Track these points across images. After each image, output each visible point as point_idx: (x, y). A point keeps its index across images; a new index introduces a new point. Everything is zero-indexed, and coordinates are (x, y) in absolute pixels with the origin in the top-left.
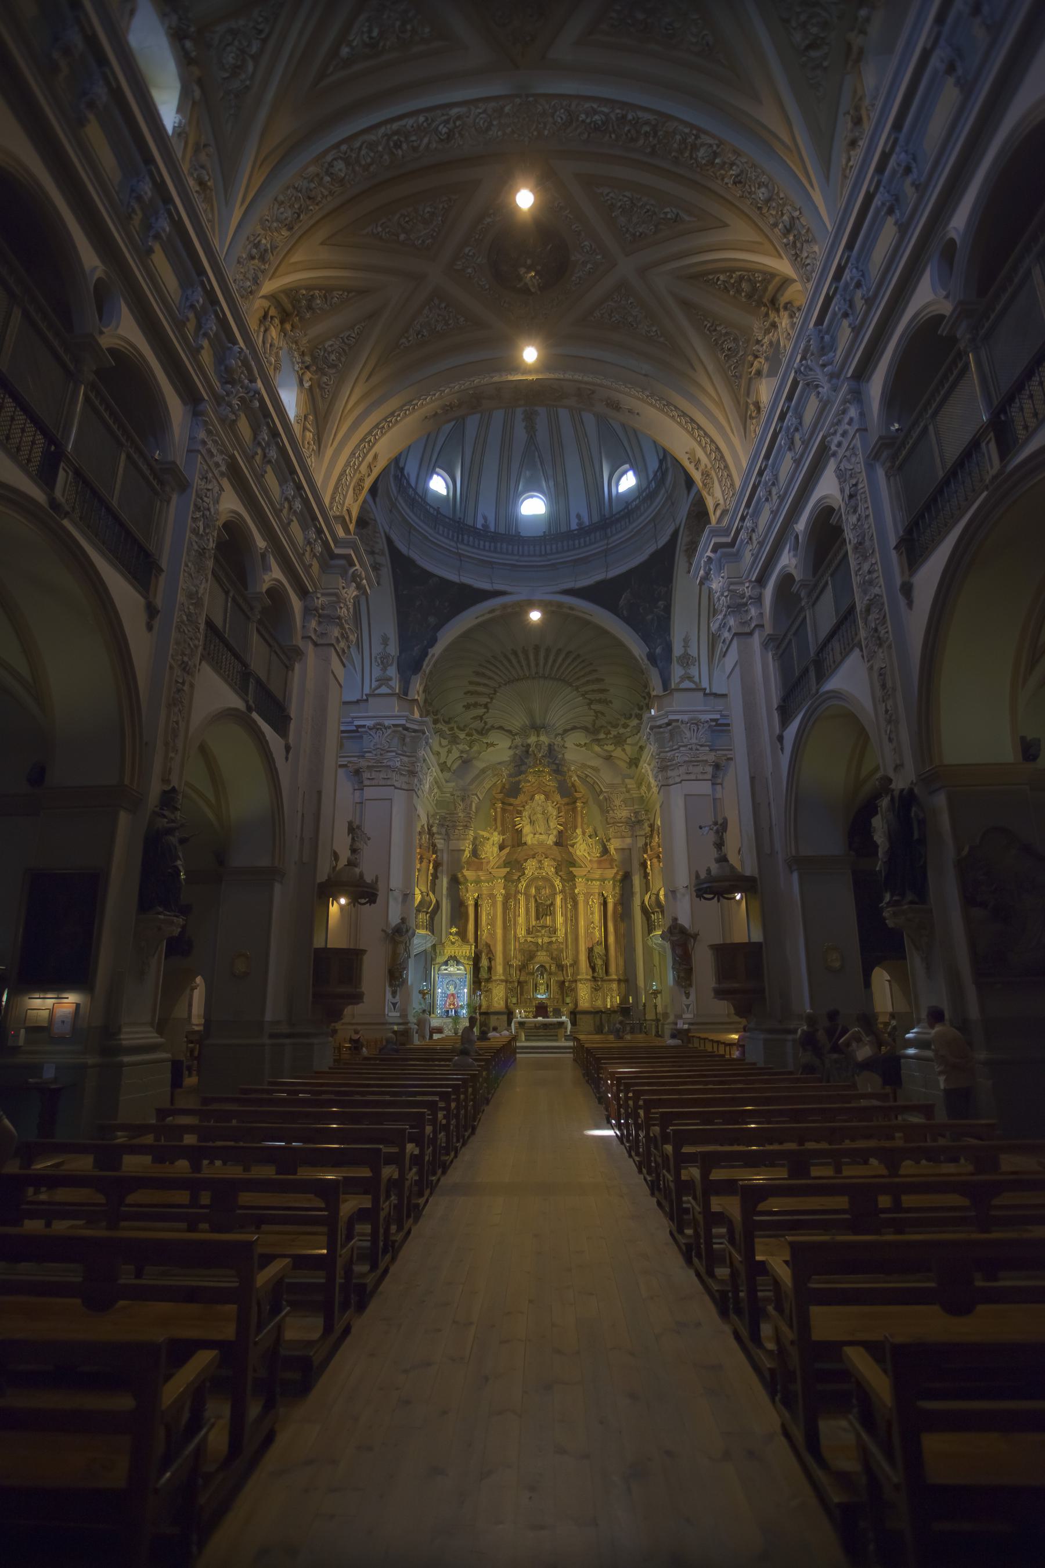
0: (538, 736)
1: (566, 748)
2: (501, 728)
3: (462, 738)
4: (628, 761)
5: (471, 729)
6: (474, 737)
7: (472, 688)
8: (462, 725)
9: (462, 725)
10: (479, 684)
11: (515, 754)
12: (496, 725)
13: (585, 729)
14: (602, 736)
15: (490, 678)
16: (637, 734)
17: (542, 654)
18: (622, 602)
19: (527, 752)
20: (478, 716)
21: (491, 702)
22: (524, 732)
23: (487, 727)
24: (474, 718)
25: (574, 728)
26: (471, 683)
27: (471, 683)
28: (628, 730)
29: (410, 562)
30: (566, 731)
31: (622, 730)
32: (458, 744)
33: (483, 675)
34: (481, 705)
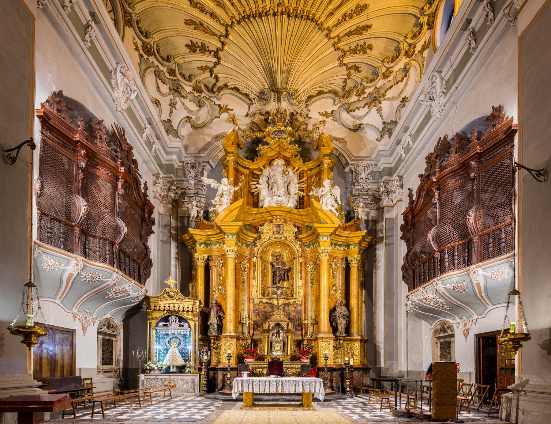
0: (279, 101)
2: (236, 89)
3: (188, 91)
6: (203, 95)
8: (187, 74)
12: (231, 84)
16: (401, 81)
19: (266, 120)
22: (262, 96)
23: (219, 84)
25: (320, 93)
28: (391, 78)
30: (310, 97)
32: (184, 97)
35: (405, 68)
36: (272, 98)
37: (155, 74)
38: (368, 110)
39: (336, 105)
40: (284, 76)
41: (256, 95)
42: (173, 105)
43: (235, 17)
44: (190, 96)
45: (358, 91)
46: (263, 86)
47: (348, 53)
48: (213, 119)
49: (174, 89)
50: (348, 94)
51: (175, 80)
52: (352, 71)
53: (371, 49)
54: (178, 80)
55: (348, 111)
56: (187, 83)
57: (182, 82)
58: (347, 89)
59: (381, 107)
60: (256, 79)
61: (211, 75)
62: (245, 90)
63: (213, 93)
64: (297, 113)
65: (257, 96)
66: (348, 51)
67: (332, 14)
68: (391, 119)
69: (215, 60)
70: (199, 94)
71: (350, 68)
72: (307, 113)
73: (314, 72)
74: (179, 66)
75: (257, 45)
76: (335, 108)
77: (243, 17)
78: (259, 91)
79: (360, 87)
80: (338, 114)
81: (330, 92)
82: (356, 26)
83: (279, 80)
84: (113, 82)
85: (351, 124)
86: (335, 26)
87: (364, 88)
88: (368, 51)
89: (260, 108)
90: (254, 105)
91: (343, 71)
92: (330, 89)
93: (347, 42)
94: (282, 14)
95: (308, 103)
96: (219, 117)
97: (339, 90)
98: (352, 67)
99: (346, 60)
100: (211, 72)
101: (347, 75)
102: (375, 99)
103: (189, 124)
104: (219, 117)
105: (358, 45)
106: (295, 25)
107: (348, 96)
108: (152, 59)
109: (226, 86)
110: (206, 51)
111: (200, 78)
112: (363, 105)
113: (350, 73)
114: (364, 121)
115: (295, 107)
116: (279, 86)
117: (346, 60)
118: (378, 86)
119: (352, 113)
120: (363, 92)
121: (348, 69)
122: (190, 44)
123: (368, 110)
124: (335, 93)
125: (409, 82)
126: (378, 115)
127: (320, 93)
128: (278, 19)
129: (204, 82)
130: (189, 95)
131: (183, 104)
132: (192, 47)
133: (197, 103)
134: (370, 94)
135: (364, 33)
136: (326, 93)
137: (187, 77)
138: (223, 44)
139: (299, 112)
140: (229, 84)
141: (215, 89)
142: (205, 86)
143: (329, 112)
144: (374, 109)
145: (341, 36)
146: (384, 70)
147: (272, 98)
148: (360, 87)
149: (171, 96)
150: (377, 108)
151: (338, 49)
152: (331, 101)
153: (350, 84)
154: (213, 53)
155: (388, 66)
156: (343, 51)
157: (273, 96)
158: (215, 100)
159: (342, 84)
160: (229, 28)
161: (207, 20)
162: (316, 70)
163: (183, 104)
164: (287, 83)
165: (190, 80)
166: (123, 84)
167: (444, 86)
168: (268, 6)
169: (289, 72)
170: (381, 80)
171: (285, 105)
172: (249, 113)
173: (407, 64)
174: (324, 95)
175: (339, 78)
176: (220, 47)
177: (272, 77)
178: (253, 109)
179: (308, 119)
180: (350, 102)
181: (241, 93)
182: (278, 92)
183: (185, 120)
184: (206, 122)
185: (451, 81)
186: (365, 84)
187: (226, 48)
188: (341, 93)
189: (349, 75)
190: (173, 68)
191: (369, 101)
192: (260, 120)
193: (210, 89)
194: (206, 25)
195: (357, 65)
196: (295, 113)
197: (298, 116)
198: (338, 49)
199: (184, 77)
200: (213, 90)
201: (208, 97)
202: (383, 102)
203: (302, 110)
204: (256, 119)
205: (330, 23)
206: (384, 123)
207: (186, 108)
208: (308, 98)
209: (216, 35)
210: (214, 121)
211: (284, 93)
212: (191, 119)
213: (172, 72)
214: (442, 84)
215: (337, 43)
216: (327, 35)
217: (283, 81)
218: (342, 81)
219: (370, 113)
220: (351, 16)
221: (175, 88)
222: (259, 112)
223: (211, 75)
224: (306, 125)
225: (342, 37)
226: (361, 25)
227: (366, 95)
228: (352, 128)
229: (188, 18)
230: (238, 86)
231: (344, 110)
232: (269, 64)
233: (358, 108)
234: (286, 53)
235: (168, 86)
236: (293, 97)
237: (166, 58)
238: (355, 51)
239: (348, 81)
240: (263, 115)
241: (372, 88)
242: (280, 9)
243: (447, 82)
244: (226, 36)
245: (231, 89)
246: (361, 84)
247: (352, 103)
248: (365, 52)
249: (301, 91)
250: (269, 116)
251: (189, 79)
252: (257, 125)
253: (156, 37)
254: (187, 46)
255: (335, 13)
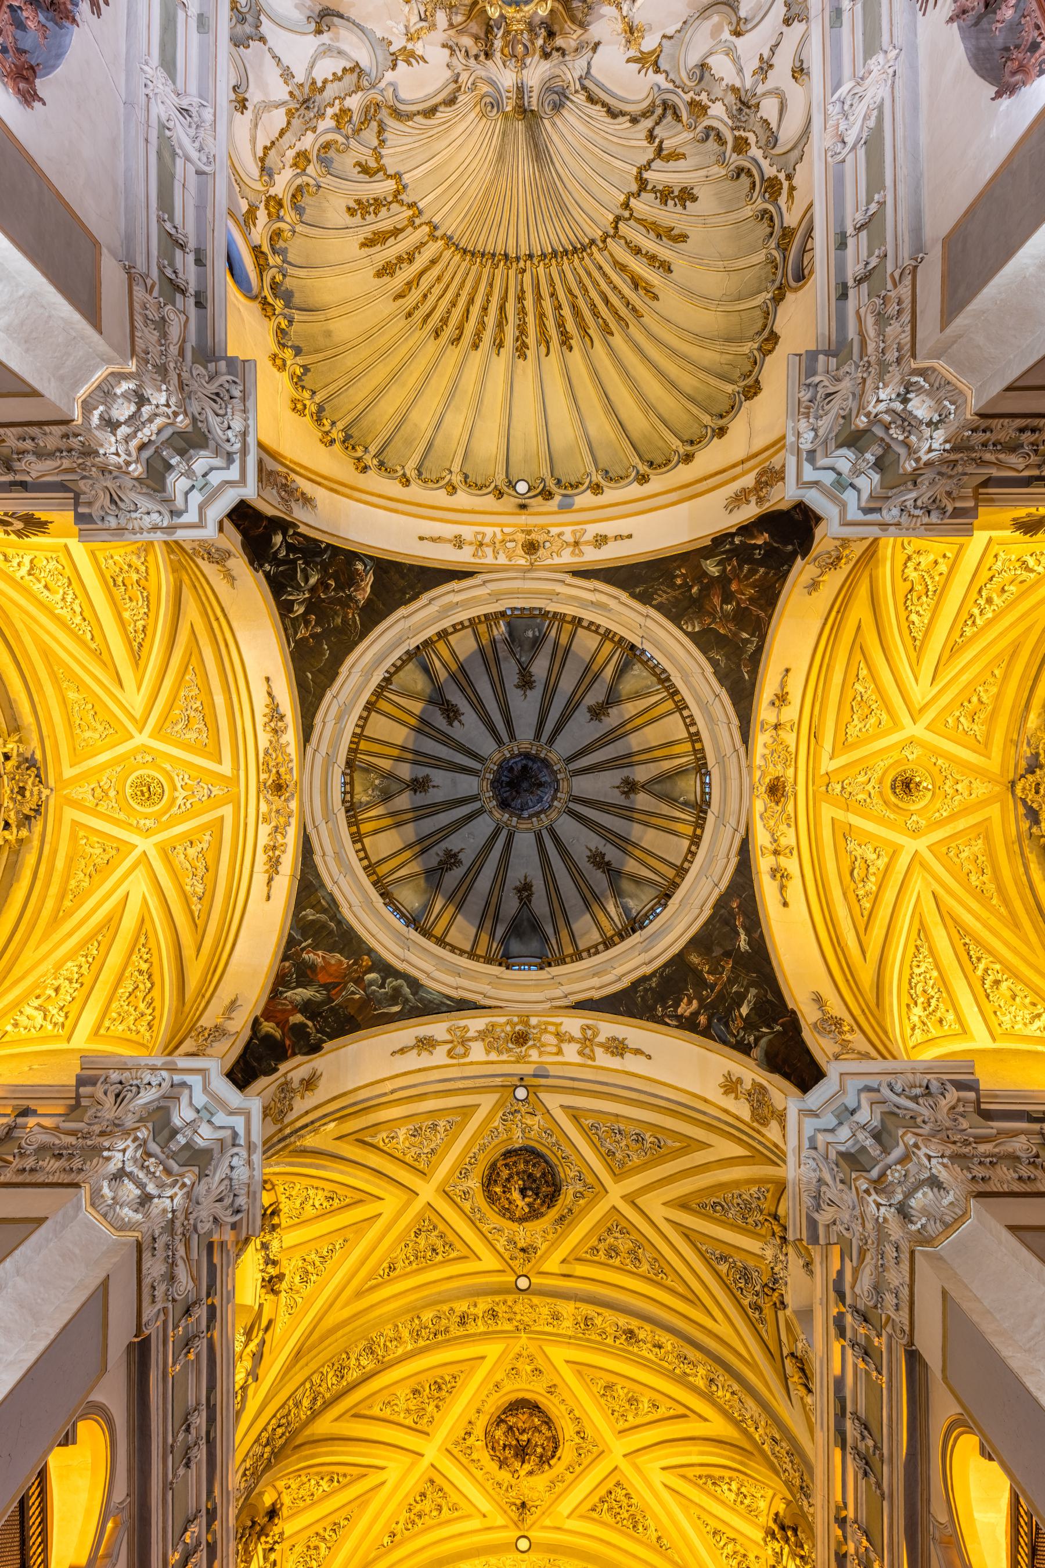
0: (520, 89)
1: (444, 46)
3: (719, 104)
4: (267, 27)
5: (689, 127)
6: (687, 97)
7: (663, 251)
9: (712, 144)
10: (652, 258)
11: (583, 25)
13: (398, 114)
14: (354, 102)
15: (622, 268)
17: (510, 331)
18: (370, 579)
20: (669, 158)
21: (630, 195)
24: (676, 156)
25: (430, 112)
26: (666, 267)
27: (666, 267)
29: (722, 677)
30: (451, 101)
31: (308, 142)
33: (636, 283)
34: (654, 190)
35: (271, 176)
36: (535, 95)
37: (776, 140)
38: (314, 75)
39: (391, 84)
40: (509, 149)
41: (572, 101)
42: (765, 67)
43: (600, 250)
44: (718, 91)
45: (350, 121)
46: (554, 124)
47: (390, 199)
48: (679, 31)
49: (749, 107)
50: (371, 111)
51: (738, 128)
52: (372, 164)
53: (349, 209)
54: (733, 129)
55: (356, 69)
56: (715, 124)
57: (726, 124)
58: (374, 125)
59: (286, 83)
60: (570, 138)
61: (661, 142)
62: (593, 113)
63: (665, 103)
64: (476, 57)
65: (568, 98)
66: (390, 203)
67: (433, 262)
68: (249, 51)
69: (646, 175)
70: (697, 98)
71: (378, 171)
72: (455, 61)
73: (451, 158)
74: (721, 160)
75: (563, 207)
76: (389, 76)
77: (584, 249)
78: (565, 112)
79: (348, 129)
80: (380, 59)
81: (410, 116)
82: (388, 244)
83: (521, 137)
84: (872, 123)
85: (343, 32)
86: (423, 244)
87: (338, 128)
88: (353, 205)
89: (564, 68)
90: (576, 76)
91: (391, 164)
92: (410, 123)
93: (396, 218)
94: (518, 259)
95: (453, 86)
96: (664, 36)
97: (391, 122)
98: (376, 173)
99: (390, 185)
100: (660, 149)
101: (382, 157)
102: (306, 103)
103: (742, 14)
104: (664, 36)
105: (376, 214)
106: (495, 243)
107: (367, 108)
108: (770, 171)
109: (634, 121)
110: (661, 192)
111: (687, 135)
112: (329, 86)
113: (378, 160)
114: (311, 43)
115: (483, 74)
116: (520, 126)
117: (390, 185)
118: (310, 136)
119: (349, 65)
120: (337, 117)
121: (381, 168)
122: (688, 203)
123: (314, 75)
124: (398, 114)
125: (249, 147)
126: (285, 61)
127: (430, 112)
128: (524, 250)
129: (680, 125)
130: (720, 95)
131: (740, 71)
132: (686, 196)
133: (707, 74)
134: (321, 115)
135: (370, 236)
136: (418, 113)
137: (711, 138)
138: (626, 205)
139: (472, 60)
140: (628, 124)
141: (659, 111)
142: (678, 118)
143: (401, 65)
144: (300, 77)
145: (410, 229)
146: (310, 170)
147: (535, 95)
148: (348, 129)
149: (760, 89)
150: (296, 80)
151: (410, 206)
152: (403, 95)
153: (370, 135)
154: (649, 187)
155: (305, 178)
156: (401, 203)
157: (534, 101)
158: (666, 85)
159: (386, 135)
160: (612, 232)
161: (648, 244)
162: (445, 163)
163: (740, 71)
164: (504, 134)
165: (709, 128)
166: (852, 118)
167: (175, 143)
168: (541, 269)
169: (501, 157)
170: (308, 148)
171: (507, 78)
172: (590, 53)
173: (271, 182)
174: (420, 107)
175: (398, 149)
176: (632, 200)
177: (536, 145)
178: (578, 66)
179: (450, 43)
180: (360, 94)
181: (604, 105)
182: (523, 111)
183: (749, 26)
184: (698, 22)
185: (167, 155)
186: (341, 139)
187: (622, 198)
188: (384, 114)
189: (379, 157)
190: (735, 155)
191: (318, 98)
192: (565, 34)
193: (669, 112)
194: (652, 235)
195: (367, 178)
196: (482, 58)
197: (474, 51)
198: (410, 206)
199: (720, 139)
200: (665, 110)
201: (679, 91)
202: (287, 97)
203: (467, 68)
204: (575, 36)
205: (432, 249)
206: (262, 39)
207: (736, 61)
208: (456, 98)
209: (639, 221)
210: (680, 24)
211: (509, 109)
212: (733, 28)
213: (741, 146)
214: (181, 147)
215: (413, 216)
216: (436, 228)
217: (511, 137)
218: (388, 143)
219: (306, 65)
220: (400, 259)
221: (746, 110)
222: (567, 58)
223: (661, 142)
224: (451, 26)
225: (407, 226)
226: (378, 248)
227: (330, 111)
228: (336, 20)
229: (682, 245)
230: (609, 120)
231: (368, 70)
232: (542, 171)
233: (337, 78)
234: (509, 193)
235: (759, 115)
236: (488, 100)
237: (743, 175)
238: (378, 203)
239: (376, 143)
240: (558, 49)
241: (320, 129)
242: (522, 264)
243: (174, 154)
244: (618, 219)
245: (623, 114)
246: (347, 138)
247: (356, 92)
248: (359, 202)
249: (473, 115)
250: (542, 48)
251: (711, 133)
252: (573, 19)
253: (748, 211)
254: (694, 199)
255: (427, 263)
